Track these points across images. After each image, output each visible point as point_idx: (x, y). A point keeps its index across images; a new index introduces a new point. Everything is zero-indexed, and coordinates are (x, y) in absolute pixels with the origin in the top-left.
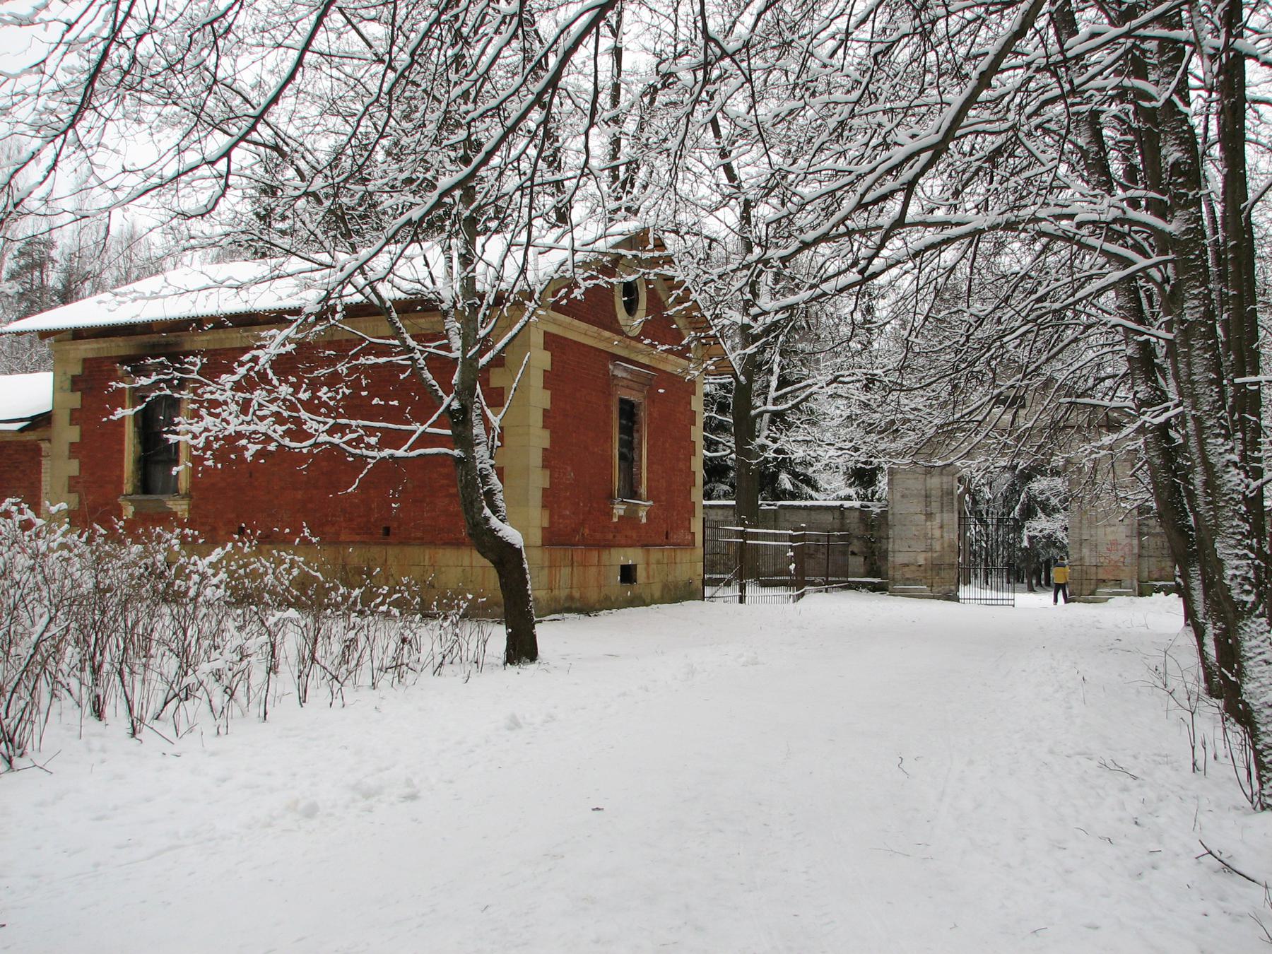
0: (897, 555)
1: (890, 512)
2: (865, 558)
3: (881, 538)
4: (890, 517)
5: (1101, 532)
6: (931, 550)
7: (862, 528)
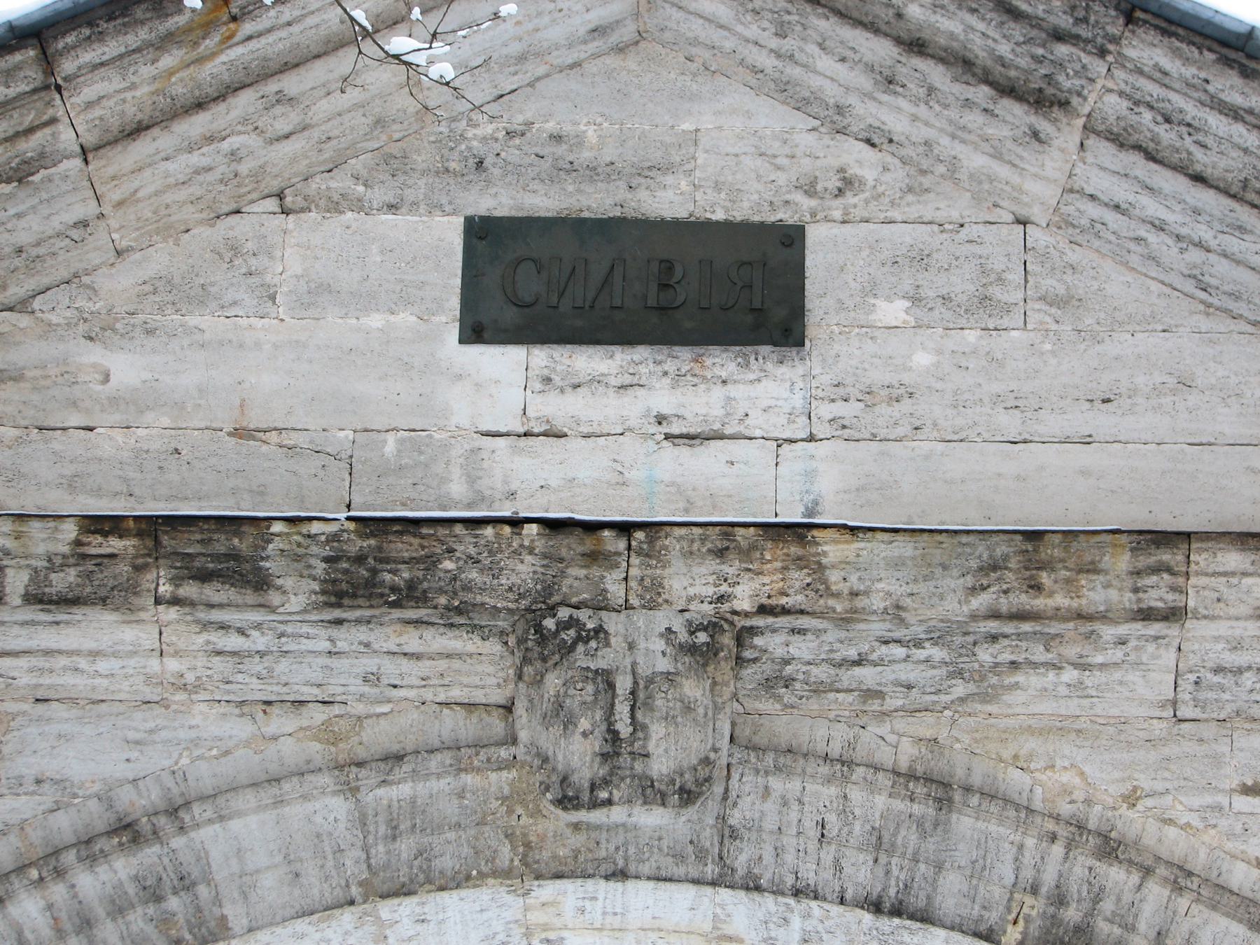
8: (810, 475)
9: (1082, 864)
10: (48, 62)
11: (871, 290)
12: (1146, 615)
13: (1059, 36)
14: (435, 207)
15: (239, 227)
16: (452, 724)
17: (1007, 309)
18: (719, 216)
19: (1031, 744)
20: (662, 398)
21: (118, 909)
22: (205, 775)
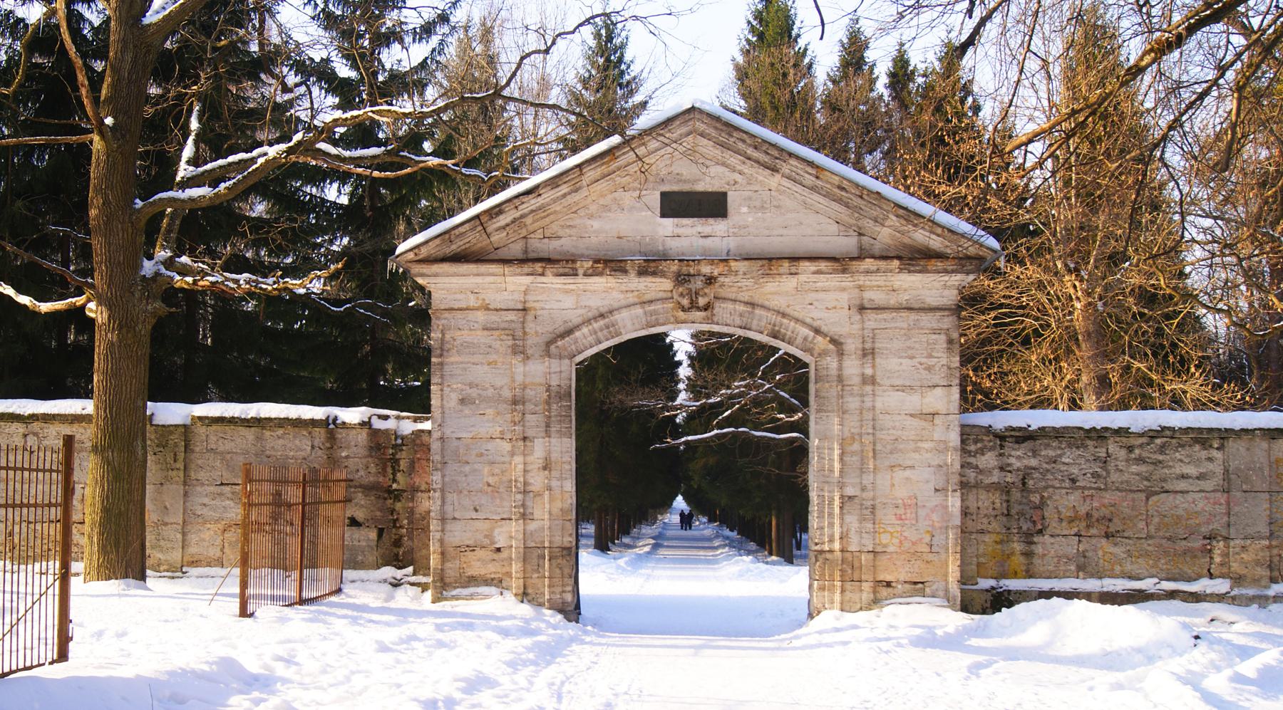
0: (448, 527)
1: (436, 435)
2: (381, 532)
3: (415, 490)
4: (435, 446)
5: (883, 480)
7: (373, 469)
10: (581, 170)
11: (740, 205)
12: (791, 274)
13: (777, 158)
14: (654, 189)
15: (616, 195)
16: (661, 295)
19: (770, 296)
20: (699, 229)
21: (601, 330)
22: (616, 305)
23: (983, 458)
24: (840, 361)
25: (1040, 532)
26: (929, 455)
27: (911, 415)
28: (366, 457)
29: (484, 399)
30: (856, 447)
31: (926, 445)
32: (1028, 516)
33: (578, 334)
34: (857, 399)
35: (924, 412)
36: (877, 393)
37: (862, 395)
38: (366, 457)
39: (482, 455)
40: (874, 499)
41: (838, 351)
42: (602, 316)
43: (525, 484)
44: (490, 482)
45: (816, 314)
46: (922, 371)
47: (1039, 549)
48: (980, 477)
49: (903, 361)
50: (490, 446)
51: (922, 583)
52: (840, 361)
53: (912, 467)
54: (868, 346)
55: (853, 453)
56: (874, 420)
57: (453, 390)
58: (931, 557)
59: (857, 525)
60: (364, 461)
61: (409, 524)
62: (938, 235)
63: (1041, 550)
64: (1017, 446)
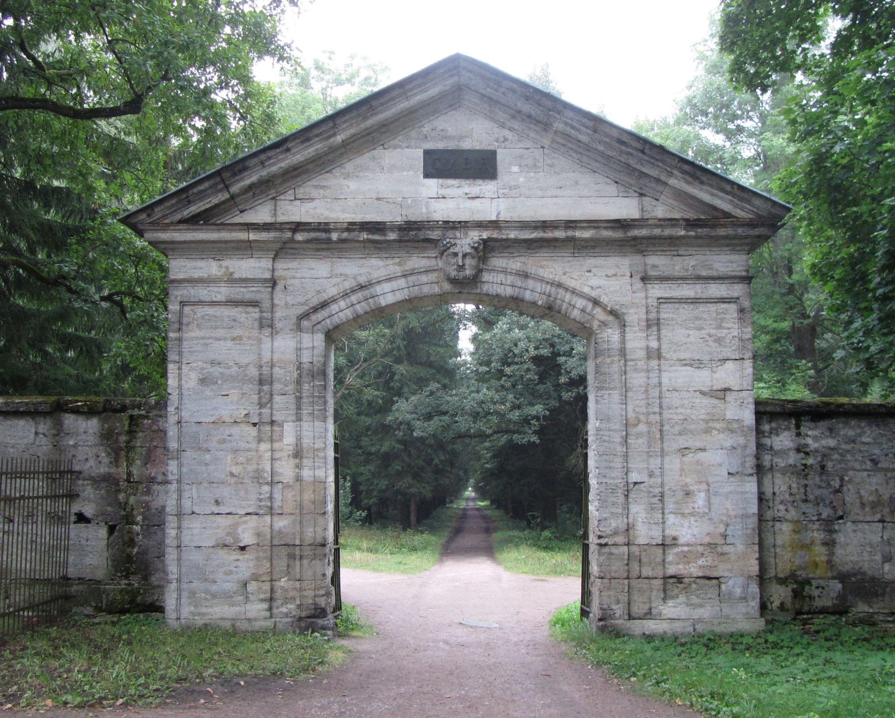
0: (185, 524)
2: (112, 530)
6: (271, 511)
7: (106, 460)
8: (498, 206)
9: (554, 289)
13: (550, 110)
14: (416, 147)
17: (539, 167)
18: (478, 148)
23: (778, 439)
24: (623, 334)
25: (841, 517)
26: (721, 436)
27: (703, 393)
28: (96, 445)
29: (225, 378)
30: (642, 428)
31: (718, 426)
32: (827, 502)
33: (334, 308)
34: (643, 374)
35: (715, 388)
36: (663, 368)
37: (648, 371)
38: (96, 445)
39: (224, 441)
40: (662, 485)
41: (620, 323)
42: (362, 287)
43: (272, 474)
44: (234, 471)
45: (594, 282)
46: (711, 343)
47: (840, 538)
48: (775, 460)
49: (691, 332)
50: (235, 430)
51: (717, 578)
52: (623, 334)
53: (703, 450)
54: (653, 316)
55: (639, 435)
56: (660, 398)
57: (192, 369)
58: (726, 549)
59: (643, 515)
60: (95, 450)
61: (144, 519)
62: (727, 193)
63: (842, 539)
64: (811, 425)
